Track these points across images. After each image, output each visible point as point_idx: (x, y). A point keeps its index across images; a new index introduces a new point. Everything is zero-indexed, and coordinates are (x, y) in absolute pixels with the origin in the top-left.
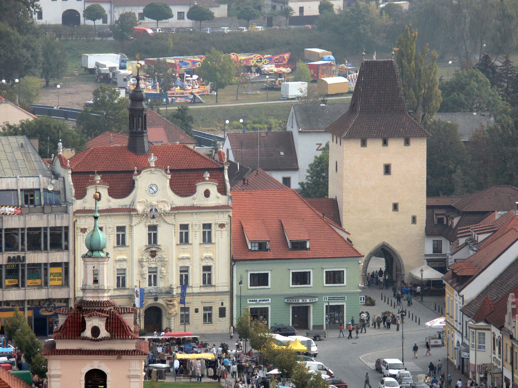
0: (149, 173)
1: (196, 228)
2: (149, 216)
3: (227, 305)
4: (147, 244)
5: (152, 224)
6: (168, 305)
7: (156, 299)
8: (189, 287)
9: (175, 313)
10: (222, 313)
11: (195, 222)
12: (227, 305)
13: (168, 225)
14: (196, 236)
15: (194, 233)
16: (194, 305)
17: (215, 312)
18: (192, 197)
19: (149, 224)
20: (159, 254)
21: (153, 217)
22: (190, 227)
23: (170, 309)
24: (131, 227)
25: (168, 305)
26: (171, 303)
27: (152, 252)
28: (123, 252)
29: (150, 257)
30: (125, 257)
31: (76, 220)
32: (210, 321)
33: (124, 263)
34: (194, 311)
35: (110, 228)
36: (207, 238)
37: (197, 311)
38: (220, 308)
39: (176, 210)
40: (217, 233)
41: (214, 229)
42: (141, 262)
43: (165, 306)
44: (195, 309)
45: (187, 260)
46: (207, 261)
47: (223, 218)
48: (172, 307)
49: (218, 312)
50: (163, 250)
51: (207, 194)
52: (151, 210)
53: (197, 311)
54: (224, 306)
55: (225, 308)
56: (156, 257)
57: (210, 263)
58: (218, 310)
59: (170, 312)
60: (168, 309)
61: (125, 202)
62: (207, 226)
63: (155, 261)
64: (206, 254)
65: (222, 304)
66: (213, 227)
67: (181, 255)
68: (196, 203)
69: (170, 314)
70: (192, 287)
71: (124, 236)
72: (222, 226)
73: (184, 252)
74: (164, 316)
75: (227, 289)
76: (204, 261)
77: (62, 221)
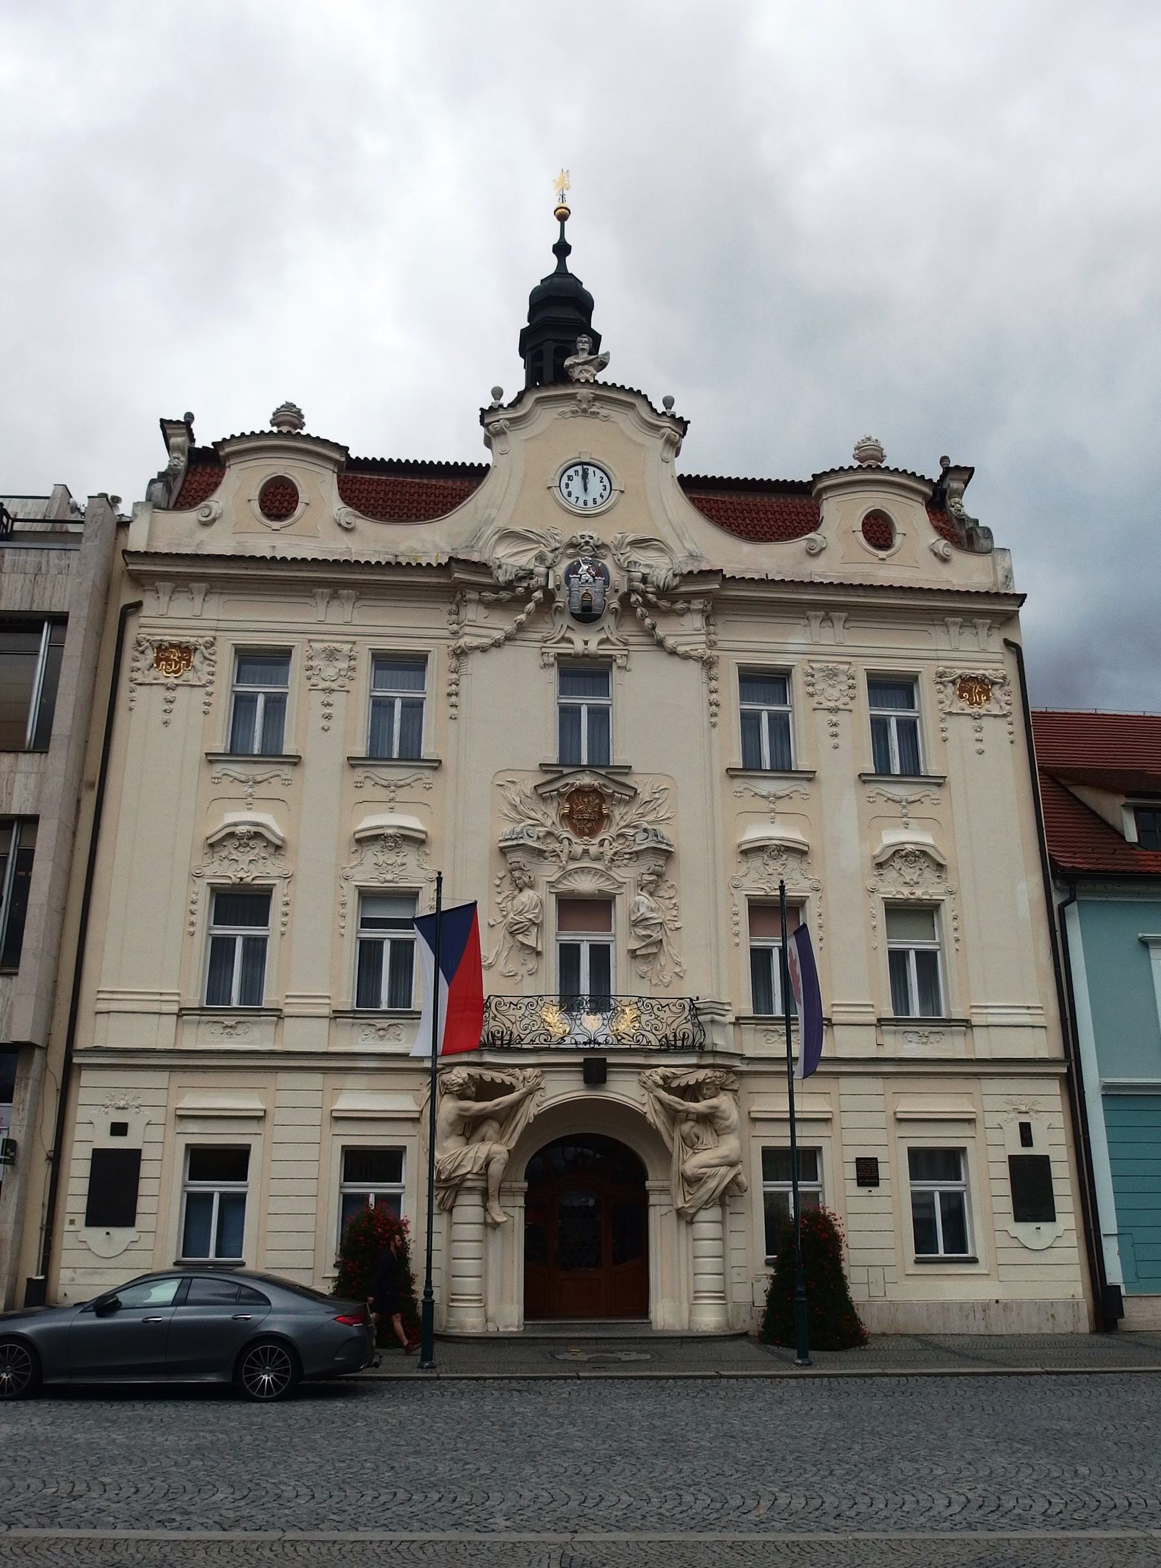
0: (568, 407)
1: (833, 694)
2: (561, 599)
3: (1053, 1142)
4: (553, 758)
5: (579, 647)
6: (674, 1116)
10: (1031, 1191)
11: (829, 664)
12: (1053, 1142)
13: (676, 660)
14: (832, 734)
15: (824, 718)
16: (849, 1137)
17: (987, 1189)
18: (799, 544)
19: (565, 648)
21: (587, 616)
22: (798, 680)
23: (691, 1143)
25: (674, 1116)
26: (701, 1106)
28: (402, 795)
29: (565, 832)
30: (411, 821)
31: (138, 605)
32: (957, 1240)
33: (410, 856)
34: (851, 1171)
35: (331, 655)
36: (898, 755)
37: (867, 1173)
38: (1015, 1162)
39: (718, 597)
40: (950, 723)
41: (930, 702)
43: (656, 1119)
44: (860, 1162)
45: (793, 863)
46: (910, 874)
47: (979, 653)
48: (708, 1137)
49: (1005, 1187)
50: (645, 796)
51: (878, 530)
52: (573, 569)
53: (867, 1173)
54: (1036, 1150)
55: (1043, 1162)
57: (927, 888)
58: (1004, 1170)
60: (675, 1146)
61: (426, 541)
62: (892, 688)
64: (893, 836)
65: (1027, 1140)
66: (927, 694)
67: (755, 832)
68: (821, 570)
69: (692, 1181)
72: (973, 687)
73: (773, 815)
74: (652, 1199)
75: (1046, 1045)
76: (890, 874)
77: (34, 582)
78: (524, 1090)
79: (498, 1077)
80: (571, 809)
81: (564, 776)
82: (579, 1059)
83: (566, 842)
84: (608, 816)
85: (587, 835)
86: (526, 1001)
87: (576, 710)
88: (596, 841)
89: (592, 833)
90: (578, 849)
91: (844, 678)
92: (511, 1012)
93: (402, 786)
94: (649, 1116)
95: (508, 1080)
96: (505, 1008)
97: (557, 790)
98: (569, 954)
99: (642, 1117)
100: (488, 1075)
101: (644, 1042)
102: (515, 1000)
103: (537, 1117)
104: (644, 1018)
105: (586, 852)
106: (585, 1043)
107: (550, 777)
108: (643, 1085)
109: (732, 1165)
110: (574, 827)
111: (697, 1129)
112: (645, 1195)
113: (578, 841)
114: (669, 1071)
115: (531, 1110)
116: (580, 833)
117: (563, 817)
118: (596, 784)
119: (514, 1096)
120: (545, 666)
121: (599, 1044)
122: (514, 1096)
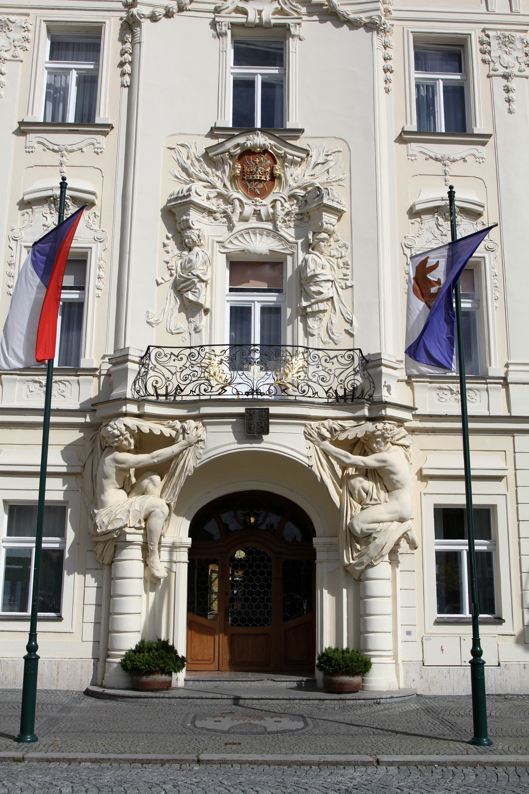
5: (252, 17)
7: (254, 421)
8: (483, 377)
9: (395, 531)
19: (240, 19)
20: (296, 177)
22: (475, 47)
24: (130, 26)
26: (370, 461)
27: (248, 152)
29: (236, 194)
42: (176, 214)
56: (278, 193)
59: (359, 527)
63: (272, 219)
70: (505, 383)
71: (89, 84)
74: (320, 556)
78: (183, 442)
79: (157, 428)
80: (242, 172)
81: (233, 137)
82: (241, 410)
83: (237, 203)
84: (280, 177)
85: (258, 195)
86: (188, 352)
87: (251, 84)
88: (267, 201)
89: (264, 194)
90: (248, 210)
91: (519, 45)
92: (171, 363)
93: (72, 151)
94: (315, 469)
95: (168, 432)
96: (165, 359)
97: (228, 151)
98: (240, 316)
99: (308, 471)
100: (146, 426)
101: (310, 394)
102: (176, 351)
103: (198, 471)
104: (312, 369)
105: (257, 214)
106: (247, 394)
107: (221, 140)
108: (308, 436)
109: (402, 520)
110: (246, 187)
111: (368, 485)
112: (313, 553)
113: (249, 202)
114: (335, 425)
115: (191, 462)
116: (252, 194)
117: (233, 179)
118: (267, 144)
119: (174, 449)
120: (220, 35)
121: (262, 394)
122: (174, 449)
